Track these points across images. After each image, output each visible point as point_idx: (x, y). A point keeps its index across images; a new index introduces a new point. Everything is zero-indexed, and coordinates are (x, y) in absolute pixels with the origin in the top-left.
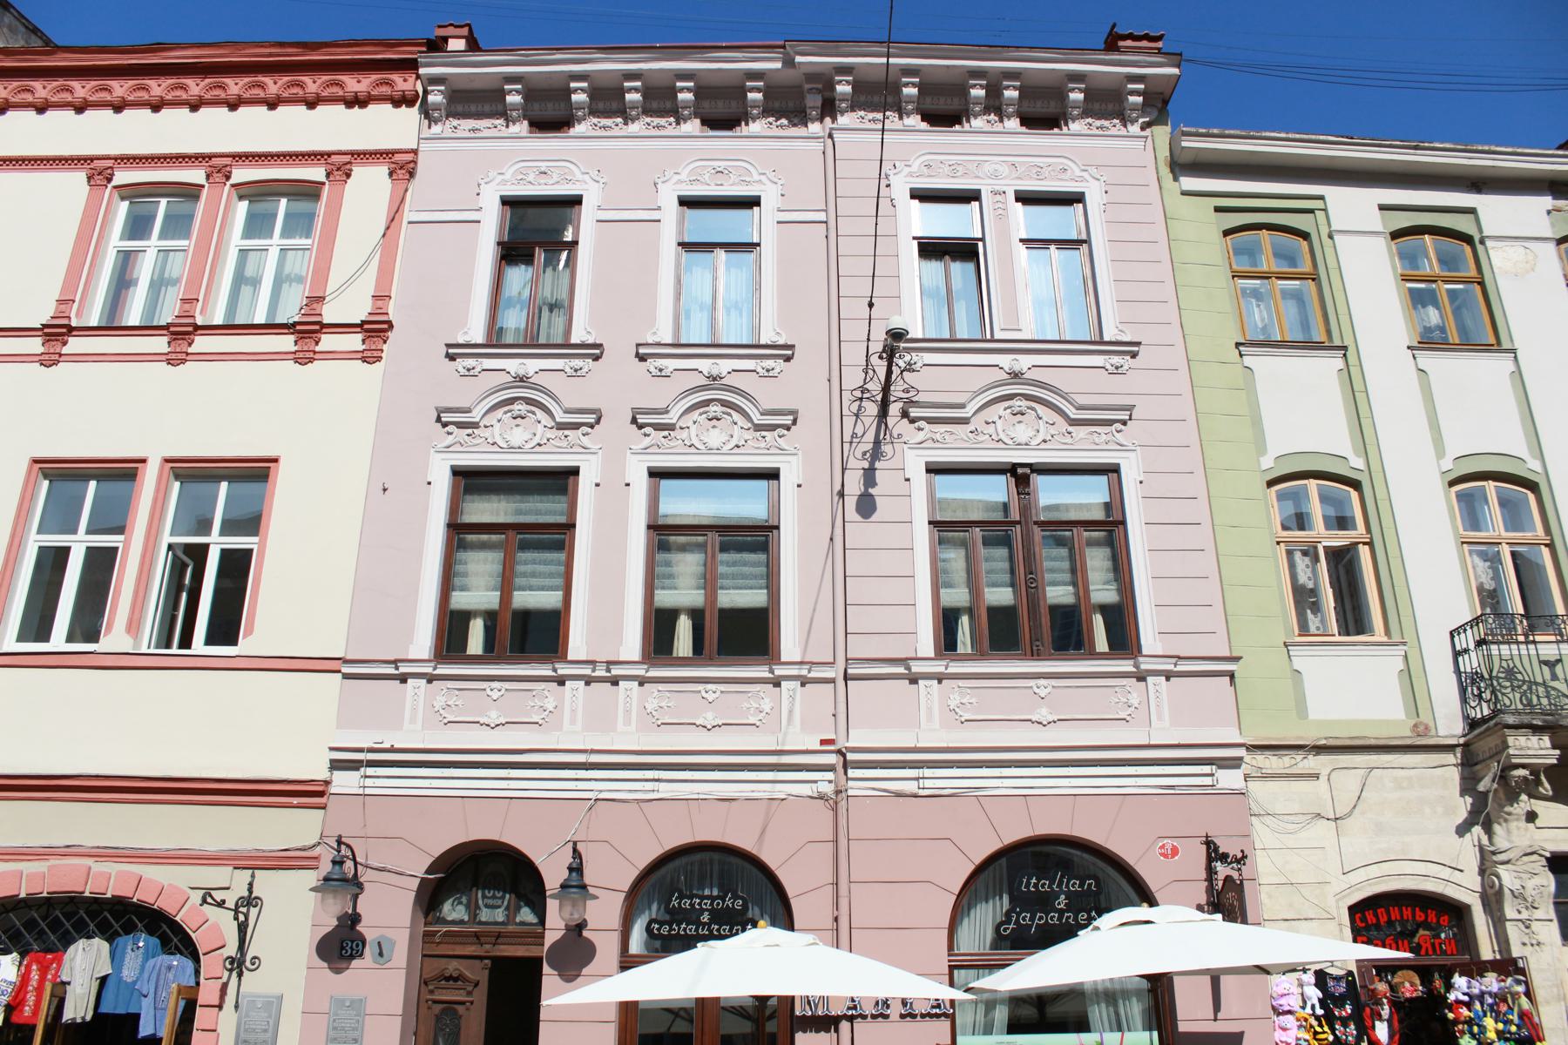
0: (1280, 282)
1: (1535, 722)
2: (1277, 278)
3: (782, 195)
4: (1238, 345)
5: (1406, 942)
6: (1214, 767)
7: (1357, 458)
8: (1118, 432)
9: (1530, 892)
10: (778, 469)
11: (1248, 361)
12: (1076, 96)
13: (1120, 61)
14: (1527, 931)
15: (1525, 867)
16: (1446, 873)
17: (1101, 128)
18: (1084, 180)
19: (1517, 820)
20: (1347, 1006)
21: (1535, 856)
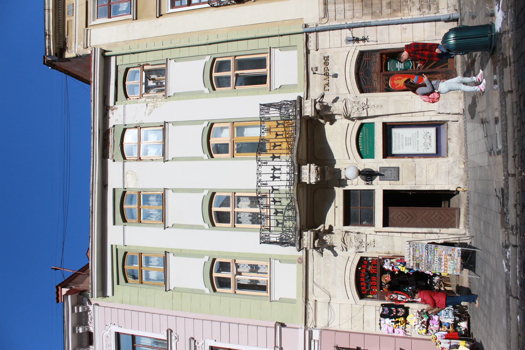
0: (143, 266)
1: (299, 239)
2: (141, 267)
3: (114, 324)
4: (166, 291)
5: (372, 278)
6: (312, 341)
7: (205, 258)
8: (198, 344)
9: (358, 244)
10: (210, 346)
11: (172, 288)
12: (81, 330)
13: (67, 317)
14: (370, 245)
15: (348, 243)
16: (349, 263)
17: (91, 319)
18: (110, 331)
19: (332, 240)
20: (393, 309)
21: (345, 238)
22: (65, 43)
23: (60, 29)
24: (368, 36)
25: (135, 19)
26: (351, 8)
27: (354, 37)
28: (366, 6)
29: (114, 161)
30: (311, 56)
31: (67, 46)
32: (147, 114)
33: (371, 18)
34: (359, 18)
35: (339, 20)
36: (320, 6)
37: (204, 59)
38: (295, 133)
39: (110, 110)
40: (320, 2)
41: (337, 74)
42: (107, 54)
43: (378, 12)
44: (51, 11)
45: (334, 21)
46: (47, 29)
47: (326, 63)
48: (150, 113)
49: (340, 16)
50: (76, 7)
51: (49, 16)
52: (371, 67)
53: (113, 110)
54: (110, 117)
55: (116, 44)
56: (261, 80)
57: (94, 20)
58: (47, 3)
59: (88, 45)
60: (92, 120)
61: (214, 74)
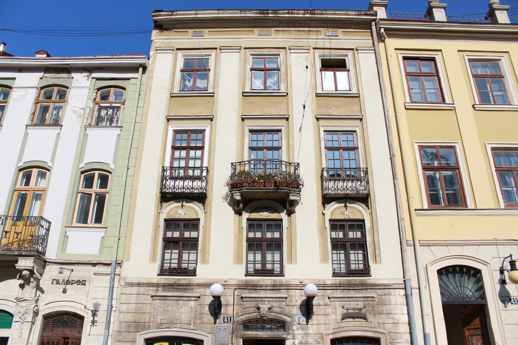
22: (167, 29)
23: (181, 25)
24: (96, 326)
25: (171, 95)
26: (130, 311)
27: (98, 311)
28: (129, 326)
29: (41, 78)
30: (90, 267)
31: (164, 32)
32: (74, 108)
33: (115, 330)
34: (118, 317)
35: (120, 297)
36: (138, 279)
37: (114, 163)
38: (4, 250)
39: (88, 74)
40: (141, 279)
41: (66, 293)
42: (141, 70)
43: (120, 337)
44: (195, 16)
45: (120, 292)
46: (178, 13)
47: (79, 282)
48: (74, 112)
49: (124, 298)
50: (198, 39)
51: (190, 15)
52: (71, 327)
53: (88, 76)
54: (82, 74)
55: (152, 77)
56: (83, 218)
57: (183, 56)
58: (203, 12)
59: (158, 52)
60: (77, 58)
61: (97, 173)
